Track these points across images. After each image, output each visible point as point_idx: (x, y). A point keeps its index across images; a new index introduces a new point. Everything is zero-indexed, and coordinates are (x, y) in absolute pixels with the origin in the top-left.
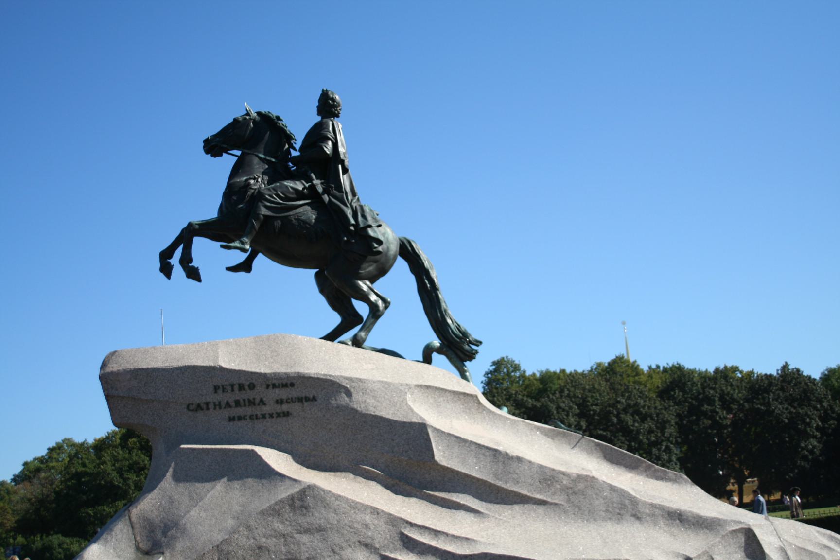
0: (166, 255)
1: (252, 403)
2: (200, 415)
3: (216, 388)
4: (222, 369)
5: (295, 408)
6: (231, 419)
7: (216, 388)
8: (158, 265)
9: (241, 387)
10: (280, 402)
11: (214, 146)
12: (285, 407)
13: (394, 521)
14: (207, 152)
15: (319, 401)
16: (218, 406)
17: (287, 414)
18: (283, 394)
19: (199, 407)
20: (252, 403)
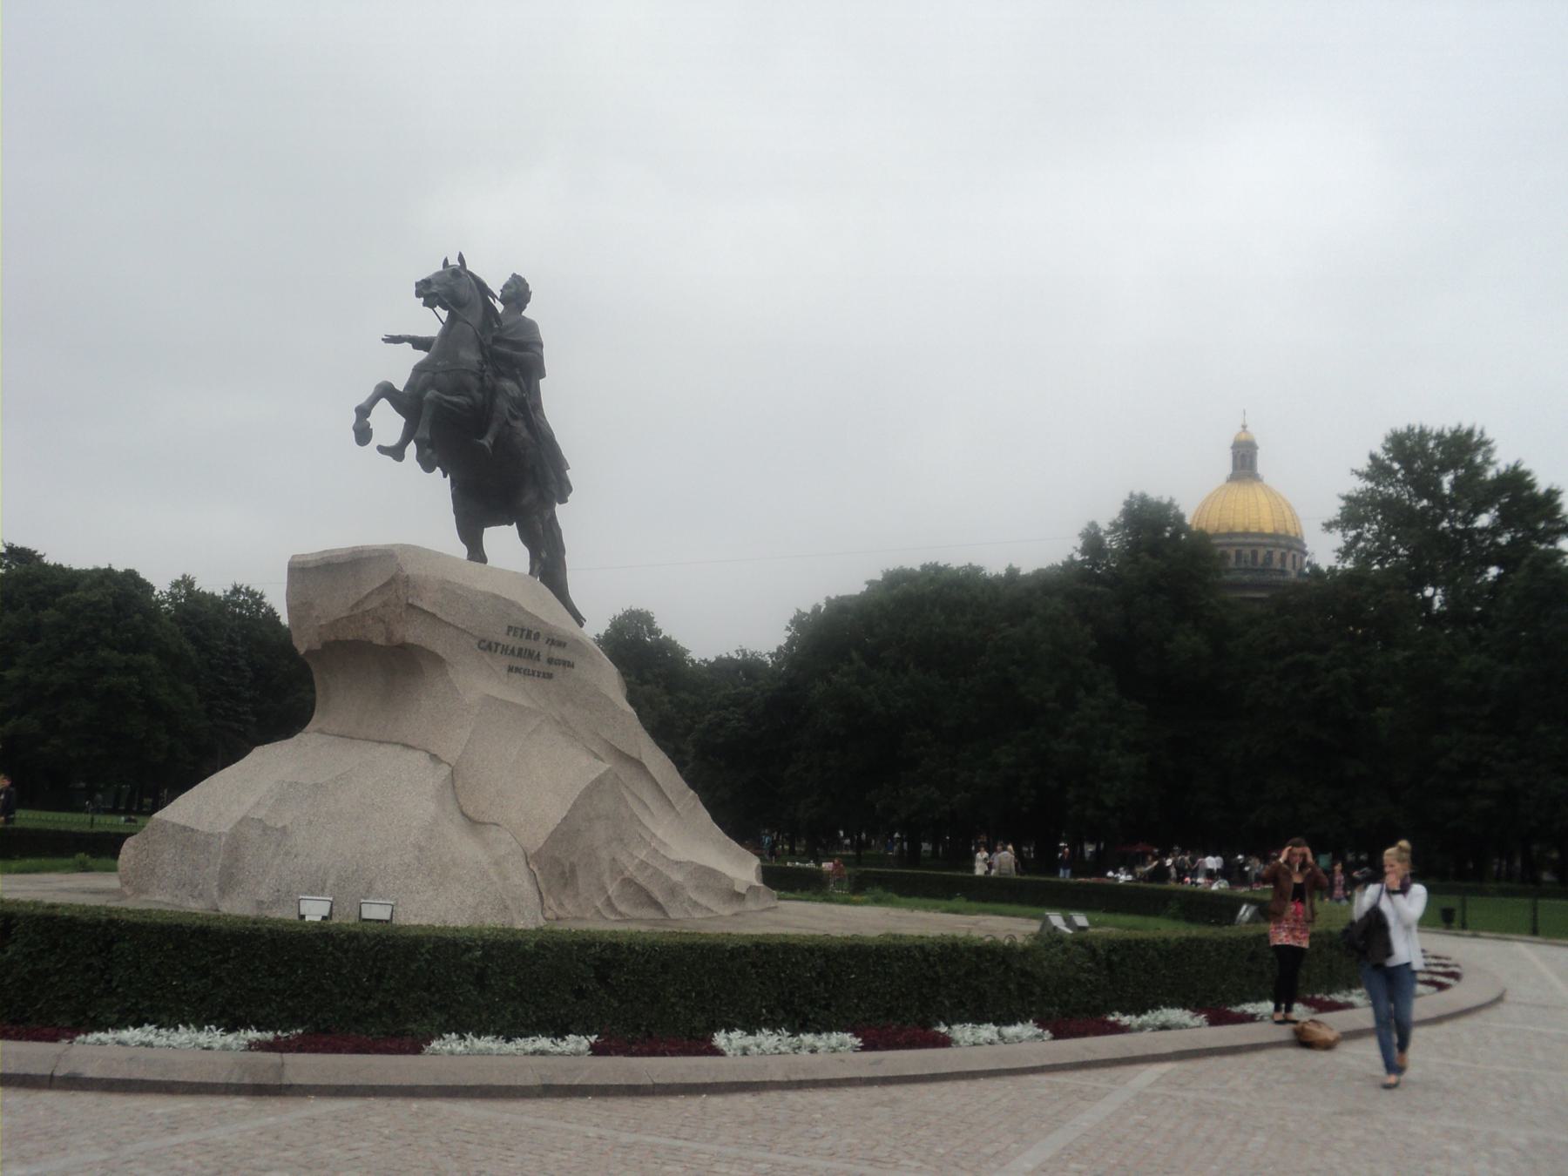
0: (363, 412)
1: (531, 655)
2: (486, 656)
3: (510, 628)
4: (521, 609)
5: (557, 670)
6: (510, 669)
7: (510, 628)
8: (353, 417)
9: (529, 632)
10: (550, 661)
11: (429, 292)
12: (552, 669)
13: (633, 815)
14: (418, 295)
15: (575, 670)
16: (505, 650)
17: (550, 676)
18: (557, 653)
19: (489, 647)
20: (531, 655)
